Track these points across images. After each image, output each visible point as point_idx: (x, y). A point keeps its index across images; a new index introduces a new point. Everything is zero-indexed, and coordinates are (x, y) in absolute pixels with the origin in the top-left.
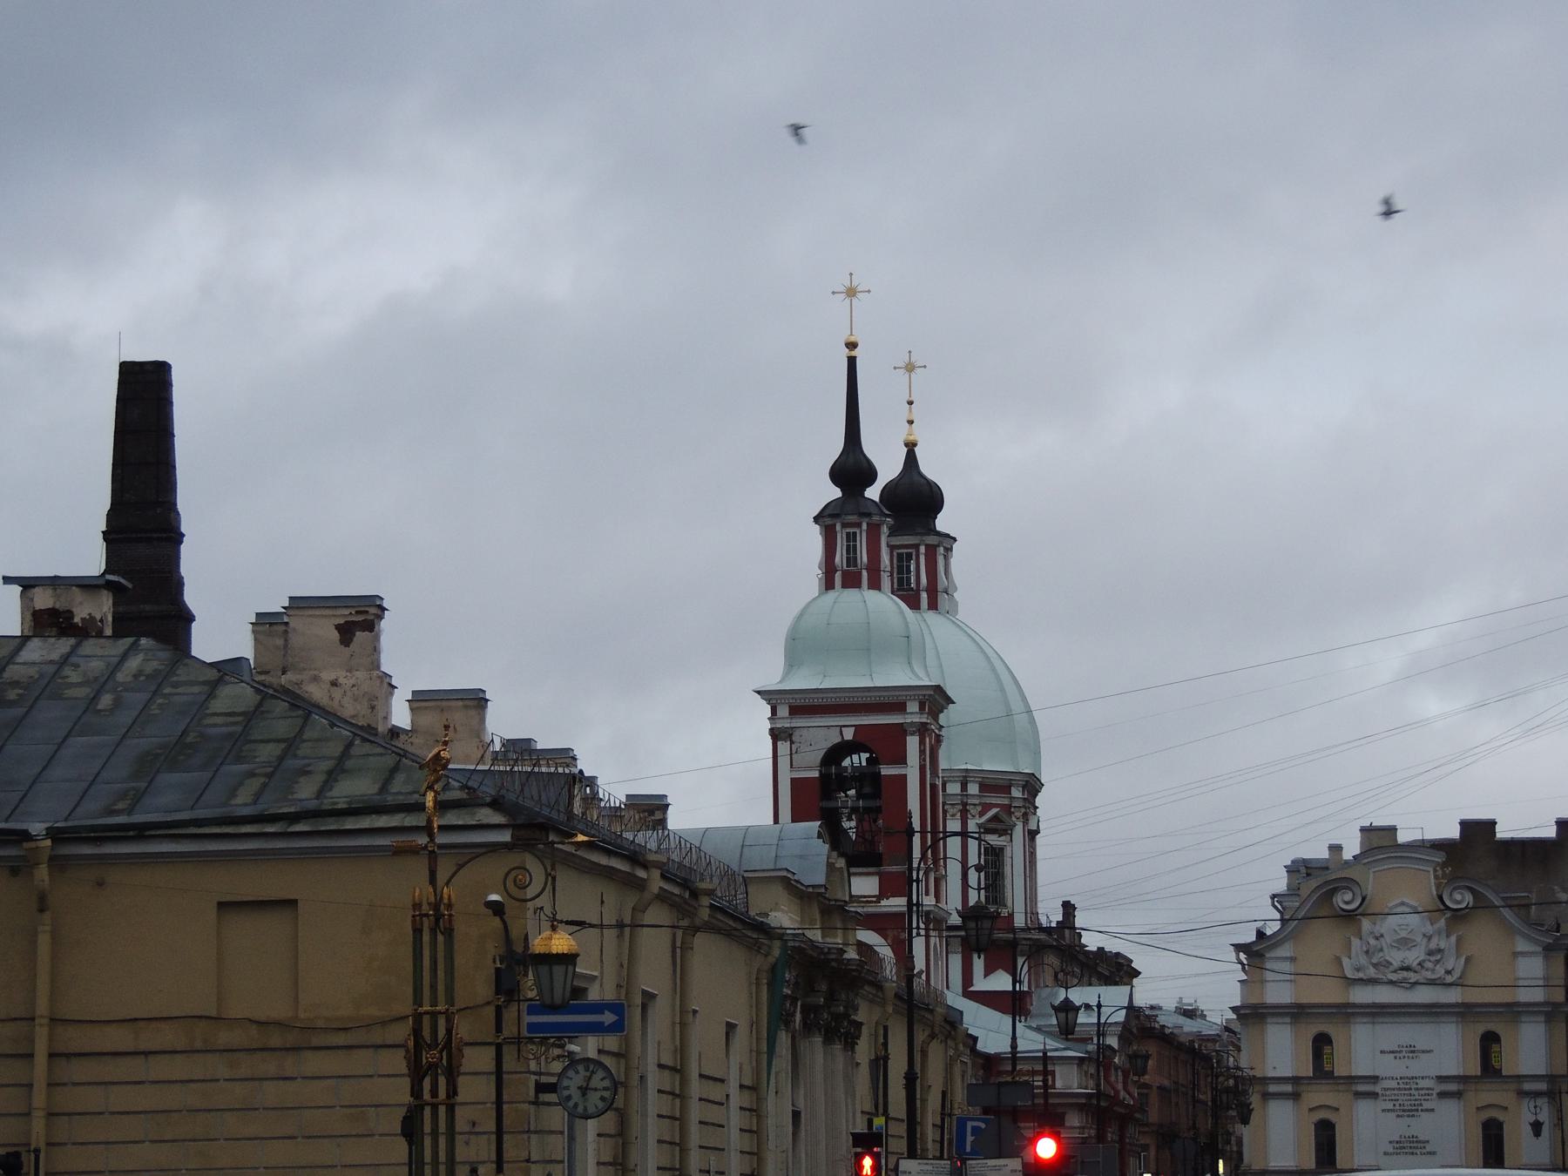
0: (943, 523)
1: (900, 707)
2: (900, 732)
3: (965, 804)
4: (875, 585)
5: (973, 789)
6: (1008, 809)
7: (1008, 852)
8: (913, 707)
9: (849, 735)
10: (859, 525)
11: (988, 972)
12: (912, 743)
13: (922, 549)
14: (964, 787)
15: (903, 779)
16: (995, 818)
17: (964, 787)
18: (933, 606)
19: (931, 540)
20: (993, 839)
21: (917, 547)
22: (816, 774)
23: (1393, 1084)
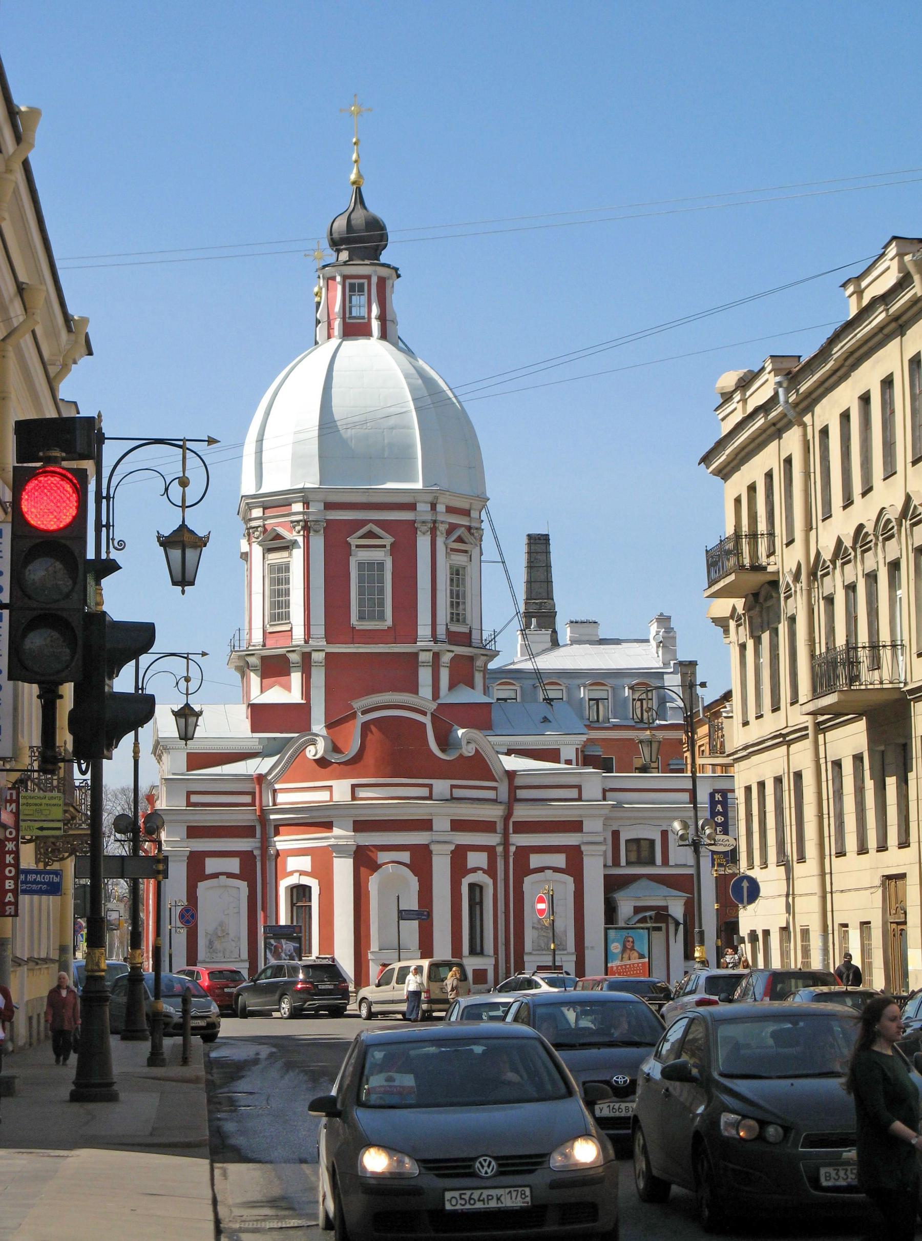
0: (385, 257)
3: (435, 522)
13: (374, 280)
14: (433, 506)
17: (433, 506)
20: (459, 559)
21: (369, 278)
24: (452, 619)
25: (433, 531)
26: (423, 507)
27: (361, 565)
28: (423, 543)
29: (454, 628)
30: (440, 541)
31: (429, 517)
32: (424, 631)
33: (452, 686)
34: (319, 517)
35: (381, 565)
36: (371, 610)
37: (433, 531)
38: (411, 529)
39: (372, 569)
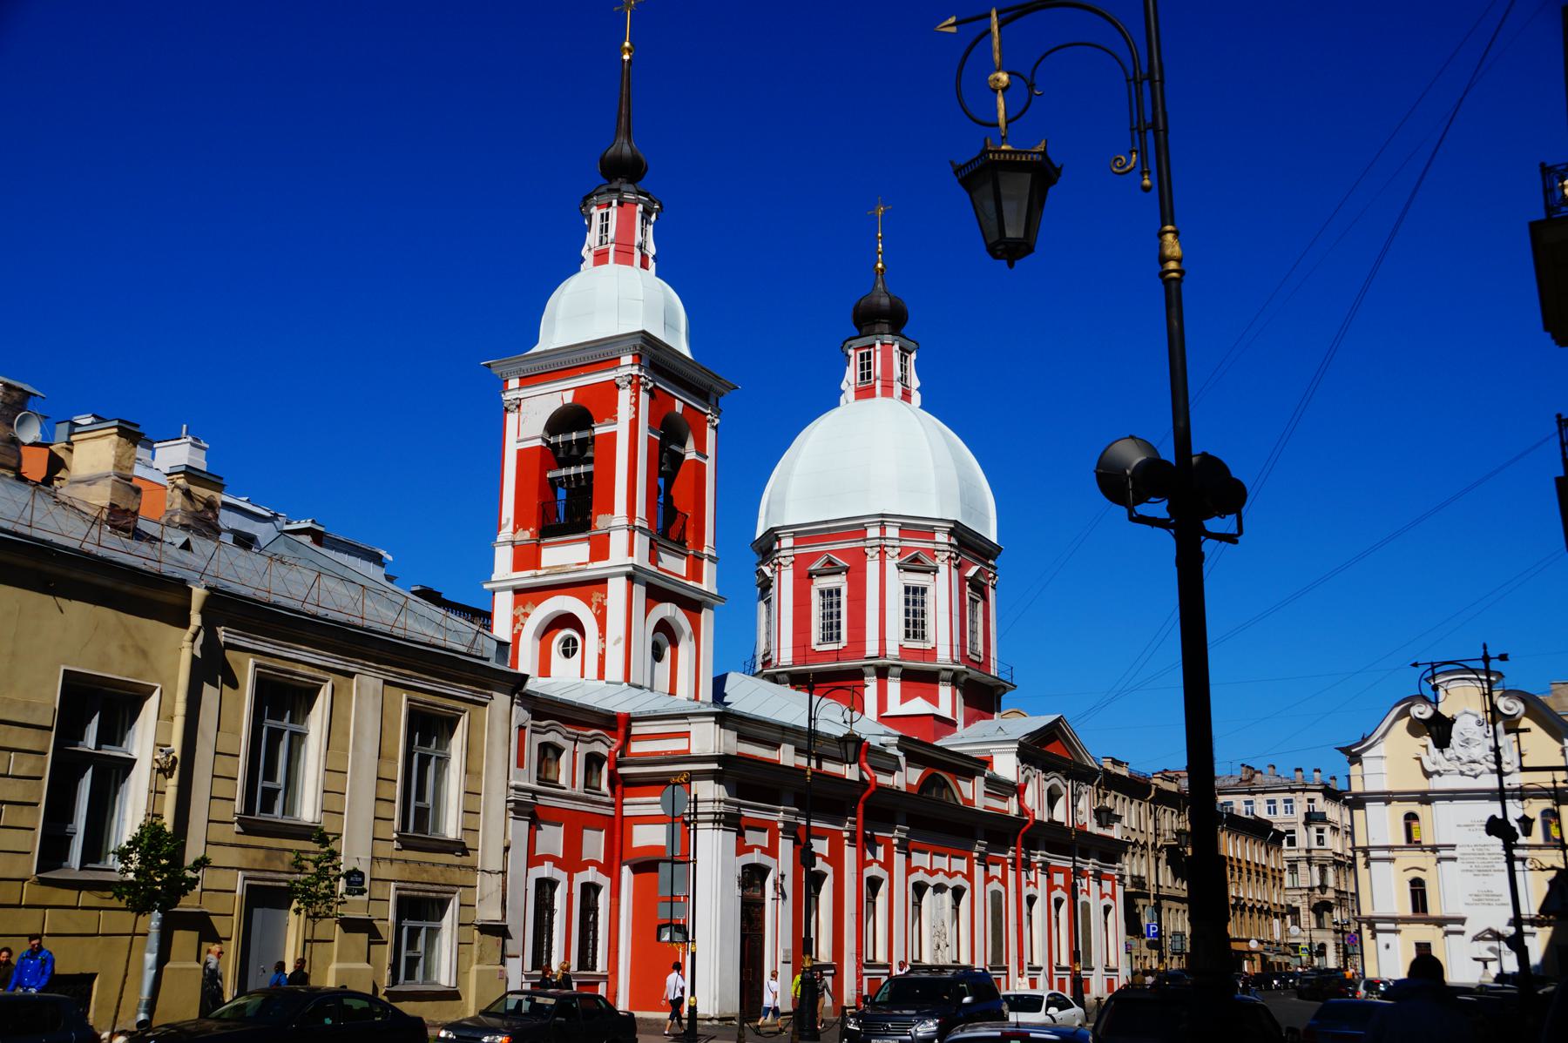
1: (614, 363)
2: (613, 387)
4: (624, 256)
5: (892, 532)
6: (932, 554)
7: (930, 591)
8: (627, 359)
9: (569, 398)
10: (610, 205)
11: (905, 698)
12: (625, 396)
15: (612, 436)
16: (915, 559)
18: (888, 390)
19: (888, 339)
22: (539, 442)
23: (1469, 850)
24: (907, 635)
25: (882, 553)
26: (873, 532)
27: (822, 593)
28: (872, 568)
29: (908, 645)
30: (891, 565)
31: (877, 542)
32: (872, 648)
33: (905, 698)
34: (790, 552)
35: (838, 592)
36: (831, 632)
37: (882, 553)
38: (861, 555)
39: (830, 594)
